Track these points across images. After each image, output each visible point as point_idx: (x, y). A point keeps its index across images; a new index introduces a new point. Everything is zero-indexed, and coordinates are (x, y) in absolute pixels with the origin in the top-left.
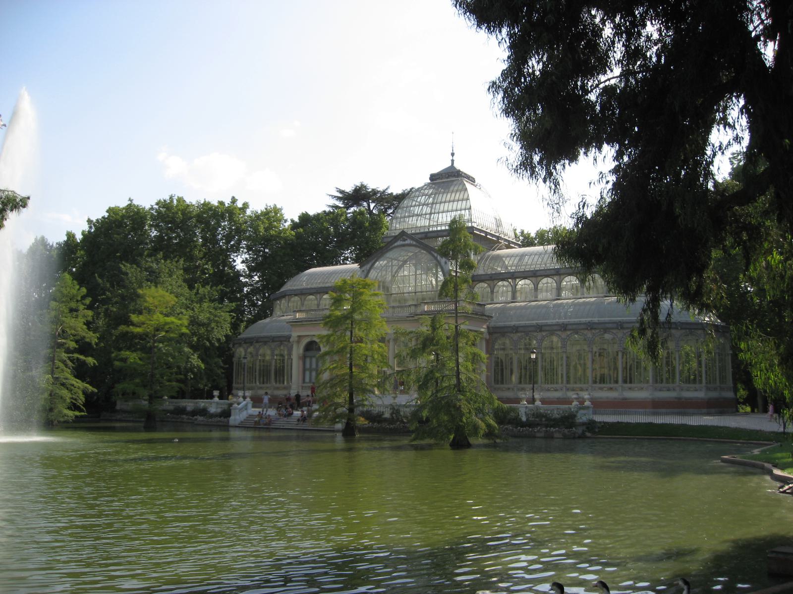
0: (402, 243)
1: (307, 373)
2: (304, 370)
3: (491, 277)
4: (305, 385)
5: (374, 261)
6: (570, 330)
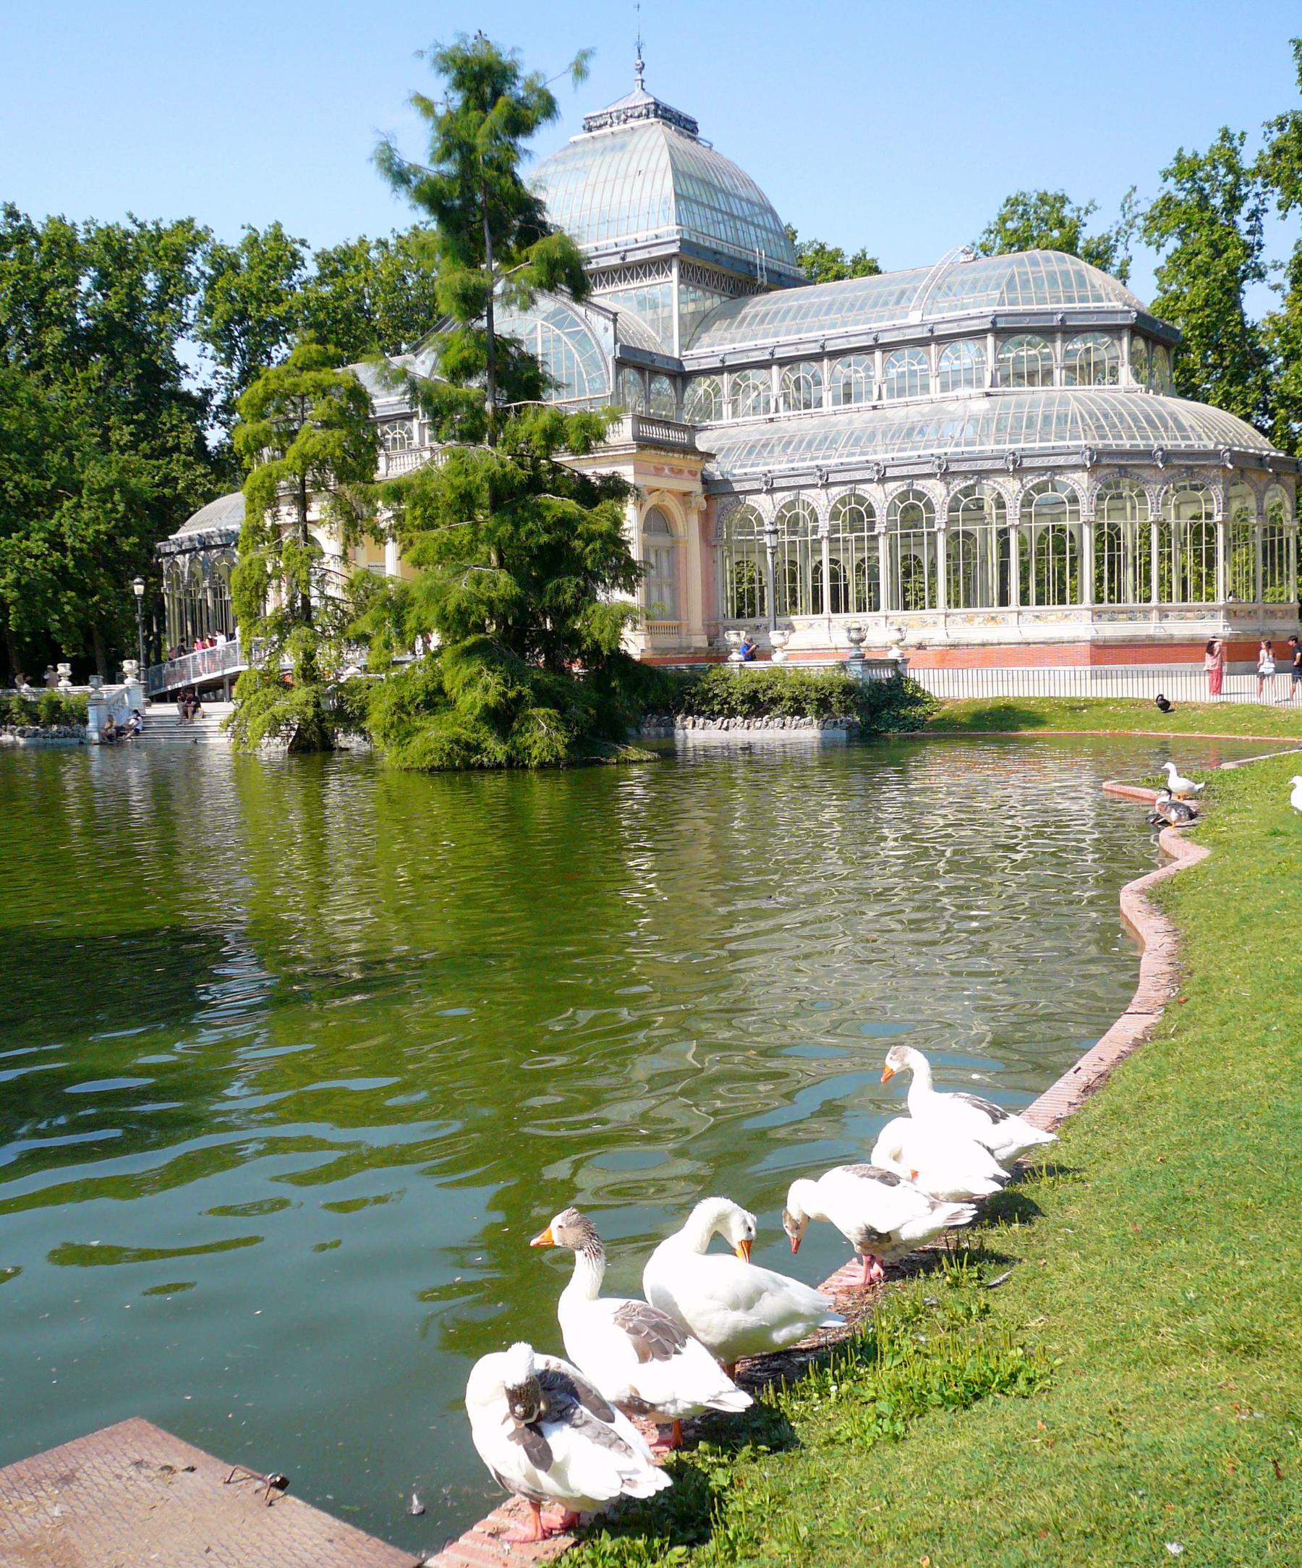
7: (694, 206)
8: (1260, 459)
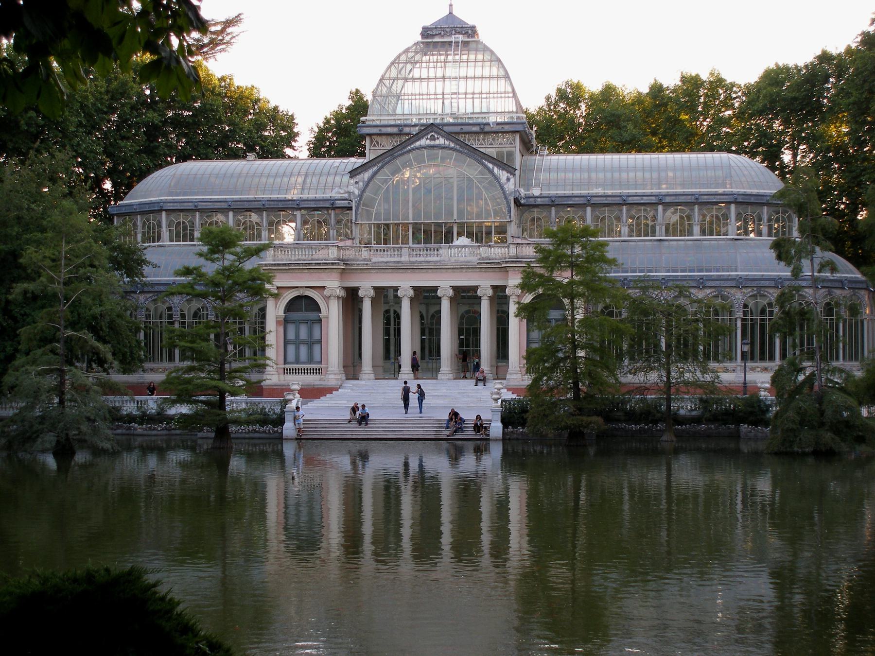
0: (428, 142)
1: (291, 349)
2: (286, 343)
4: (287, 366)
6: (711, 287)
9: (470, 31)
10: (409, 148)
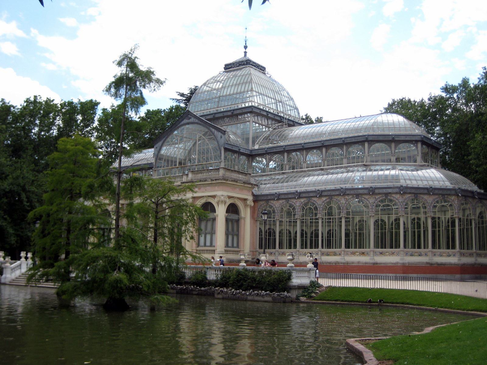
3: (266, 151)
5: (165, 138)
6: (326, 196)
7: (266, 98)
8: (472, 192)
9: (245, 63)
10: (179, 125)
